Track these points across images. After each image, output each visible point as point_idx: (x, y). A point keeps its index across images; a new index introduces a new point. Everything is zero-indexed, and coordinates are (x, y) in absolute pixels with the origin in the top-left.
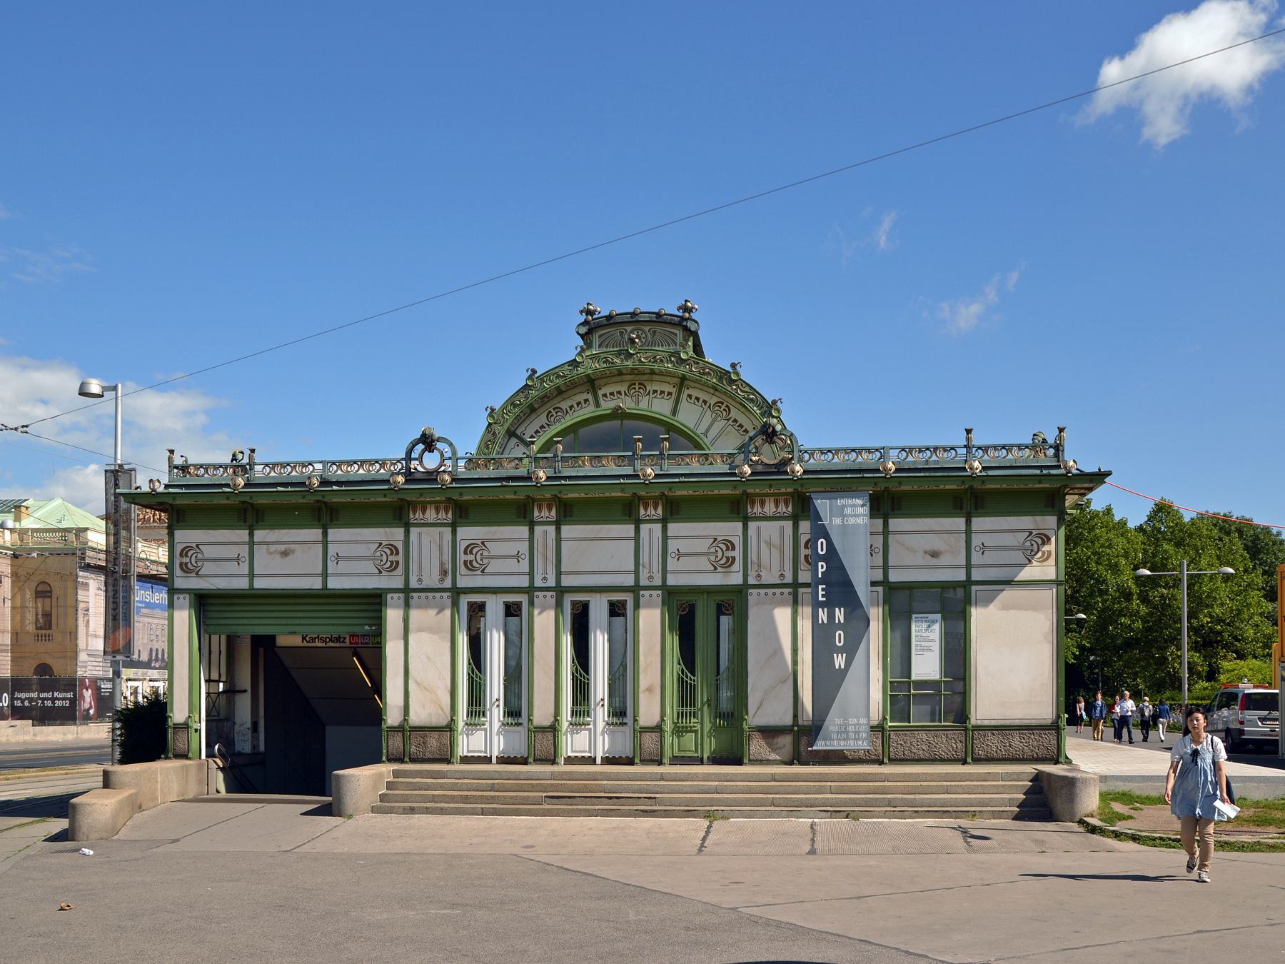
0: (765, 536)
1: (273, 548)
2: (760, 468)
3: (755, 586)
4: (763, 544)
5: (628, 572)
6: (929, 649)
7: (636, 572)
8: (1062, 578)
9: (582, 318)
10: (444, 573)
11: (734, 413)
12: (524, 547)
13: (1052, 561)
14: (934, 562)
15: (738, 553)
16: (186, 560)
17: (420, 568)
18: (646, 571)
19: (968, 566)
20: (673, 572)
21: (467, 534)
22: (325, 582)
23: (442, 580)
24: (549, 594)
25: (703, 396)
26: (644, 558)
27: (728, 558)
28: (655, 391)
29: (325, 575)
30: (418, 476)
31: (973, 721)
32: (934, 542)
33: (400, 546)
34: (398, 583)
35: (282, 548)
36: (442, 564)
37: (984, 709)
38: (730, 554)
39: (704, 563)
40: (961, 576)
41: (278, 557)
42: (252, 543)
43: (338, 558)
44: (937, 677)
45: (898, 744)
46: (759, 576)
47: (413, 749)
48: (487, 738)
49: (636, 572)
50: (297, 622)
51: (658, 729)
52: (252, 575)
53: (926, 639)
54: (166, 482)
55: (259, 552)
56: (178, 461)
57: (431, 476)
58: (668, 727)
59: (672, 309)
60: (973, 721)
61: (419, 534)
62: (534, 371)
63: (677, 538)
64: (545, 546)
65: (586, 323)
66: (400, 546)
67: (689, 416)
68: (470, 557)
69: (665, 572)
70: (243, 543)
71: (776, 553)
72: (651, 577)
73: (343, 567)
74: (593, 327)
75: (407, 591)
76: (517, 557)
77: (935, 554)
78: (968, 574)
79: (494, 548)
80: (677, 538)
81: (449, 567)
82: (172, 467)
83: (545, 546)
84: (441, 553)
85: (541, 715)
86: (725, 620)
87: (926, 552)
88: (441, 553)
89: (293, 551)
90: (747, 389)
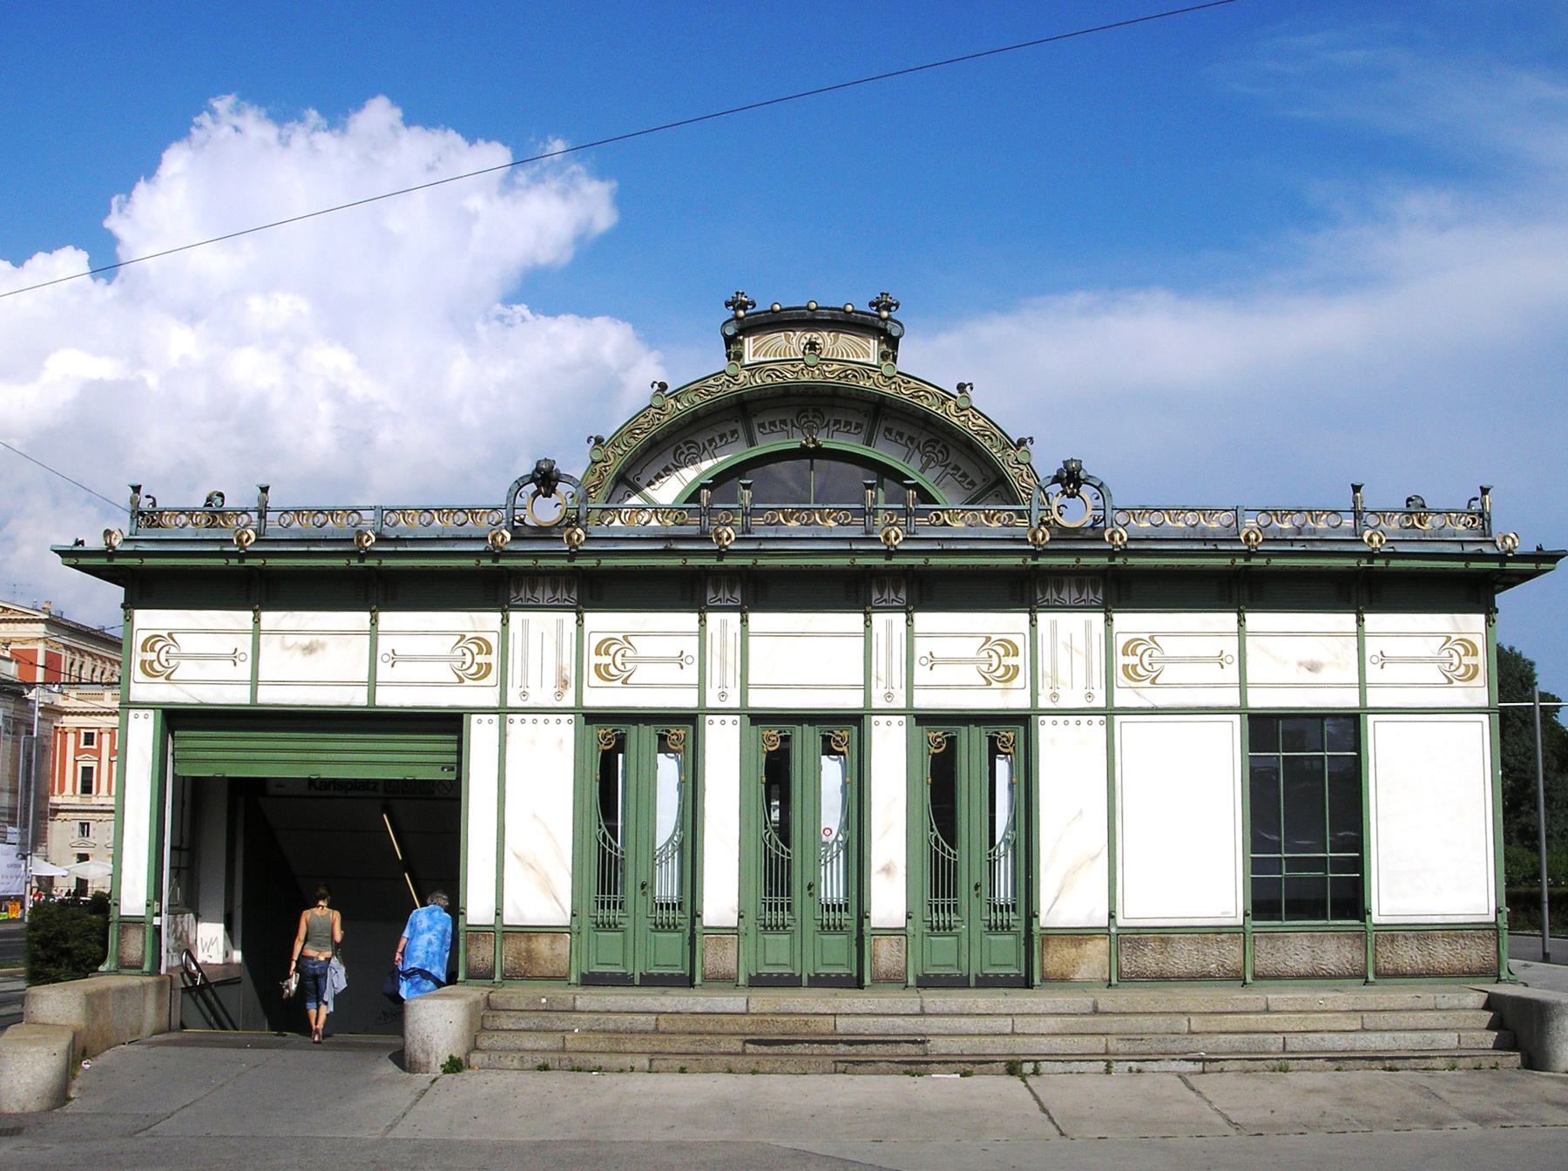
0: (1063, 636)
1: (290, 640)
4: (1061, 648)
5: (853, 687)
9: (730, 313)
11: (954, 458)
12: (691, 647)
13: (1481, 679)
15: (1022, 661)
16: (152, 656)
17: (525, 675)
18: (882, 684)
19: (1362, 686)
20: (926, 687)
21: (601, 622)
22: (372, 695)
23: (559, 694)
26: (879, 667)
27: (1007, 668)
29: (372, 684)
30: (526, 532)
33: (494, 640)
34: (490, 698)
35: (305, 640)
36: (560, 670)
38: (1010, 661)
41: (299, 653)
42: (257, 633)
43: (395, 658)
45: (1267, 957)
46: (1055, 695)
49: (867, 687)
50: (324, 757)
52: (255, 682)
54: (126, 535)
55: (268, 645)
56: (145, 504)
60: (1376, 918)
61: (525, 623)
63: (929, 635)
64: (724, 644)
66: (494, 640)
70: (244, 632)
71: (1080, 660)
72: (889, 695)
73: (403, 671)
75: (503, 711)
77: (1313, 667)
78: (1363, 696)
79: (643, 646)
80: (929, 635)
81: (571, 673)
82: (137, 513)
83: (724, 644)
86: (1002, 766)
87: (1300, 664)
89: (323, 646)
90: (980, 422)
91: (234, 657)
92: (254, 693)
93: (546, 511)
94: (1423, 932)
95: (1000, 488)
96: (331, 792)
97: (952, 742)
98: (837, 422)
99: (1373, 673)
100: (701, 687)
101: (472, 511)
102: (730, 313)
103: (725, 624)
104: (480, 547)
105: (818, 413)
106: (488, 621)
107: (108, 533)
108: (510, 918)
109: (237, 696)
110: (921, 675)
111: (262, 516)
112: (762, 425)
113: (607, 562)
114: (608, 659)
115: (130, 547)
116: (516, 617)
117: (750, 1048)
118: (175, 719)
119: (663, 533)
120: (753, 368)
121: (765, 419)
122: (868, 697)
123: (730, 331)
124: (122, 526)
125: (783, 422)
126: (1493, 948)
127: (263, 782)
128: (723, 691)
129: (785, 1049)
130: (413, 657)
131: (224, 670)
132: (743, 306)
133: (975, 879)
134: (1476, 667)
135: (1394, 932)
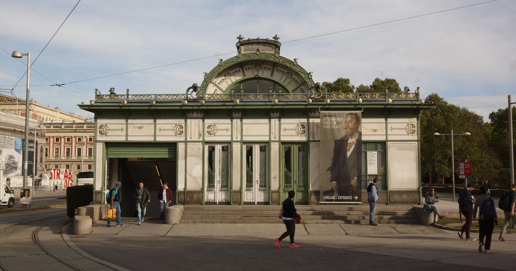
1: (135, 126)
2: (314, 99)
3: (312, 141)
5: (267, 136)
6: (373, 164)
7: (270, 136)
8: (419, 139)
9: (238, 40)
10: (200, 135)
11: (294, 76)
12: (229, 126)
13: (416, 133)
14: (375, 133)
17: (191, 133)
19: (386, 135)
20: (283, 136)
21: (208, 122)
22: (155, 138)
23: (199, 138)
24: (238, 143)
25: (282, 70)
26: (273, 130)
28: (265, 68)
29: (155, 136)
30: (191, 100)
31: (389, 189)
32: (375, 126)
34: (183, 139)
35: (139, 126)
36: (199, 132)
37: (394, 185)
39: (294, 133)
40: (383, 138)
41: (137, 129)
44: (376, 173)
46: (313, 137)
47: (188, 199)
48: (218, 195)
49: (270, 136)
50: (144, 153)
51: (278, 192)
52: (127, 136)
53: (372, 160)
57: (195, 100)
58: (281, 191)
59: (271, 38)
60: (389, 189)
61: (191, 122)
62: (222, 60)
63: (284, 124)
64: (237, 126)
65: (239, 42)
67: (277, 77)
68: (209, 130)
69: (280, 135)
73: (162, 133)
74: (242, 43)
75: (186, 142)
76: (227, 130)
77: (375, 131)
78: (387, 138)
80: (284, 124)
81: (202, 133)
83: (237, 126)
84: (199, 128)
85: (236, 186)
88: (199, 128)
89: (143, 127)
91: (122, 130)
92: (127, 138)
93: (194, 95)
94: (400, 193)
95: (305, 84)
96: (143, 160)
97: (290, 148)
98: (265, 68)
99: (389, 132)
100: (232, 136)
101: (178, 95)
102: (238, 40)
103: (237, 122)
104: (180, 104)
105: (260, 66)
106: (182, 121)
107: (91, 101)
108: (189, 188)
109: (123, 139)
110: (282, 133)
111: (128, 97)
112: (246, 69)
113: (209, 108)
114: (210, 130)
115: (96, 104)
116: (189, 121)
117: (244, 218)
118: (108, 145)
119: (223, 100)
120: (244, 55)
121: (247, 67)
122: (270, 138)
123: (238, 45)
124: (93, 98)
125: (251, 68)
126: (418, 197)
127: (126, 159)
128: (237, 137)
129: (251, 218)
130: (165, 130)
131: (120, 133)
132: (242, 39)
133: (295, 180)
134: (415, 131)
135: (392, 192)
